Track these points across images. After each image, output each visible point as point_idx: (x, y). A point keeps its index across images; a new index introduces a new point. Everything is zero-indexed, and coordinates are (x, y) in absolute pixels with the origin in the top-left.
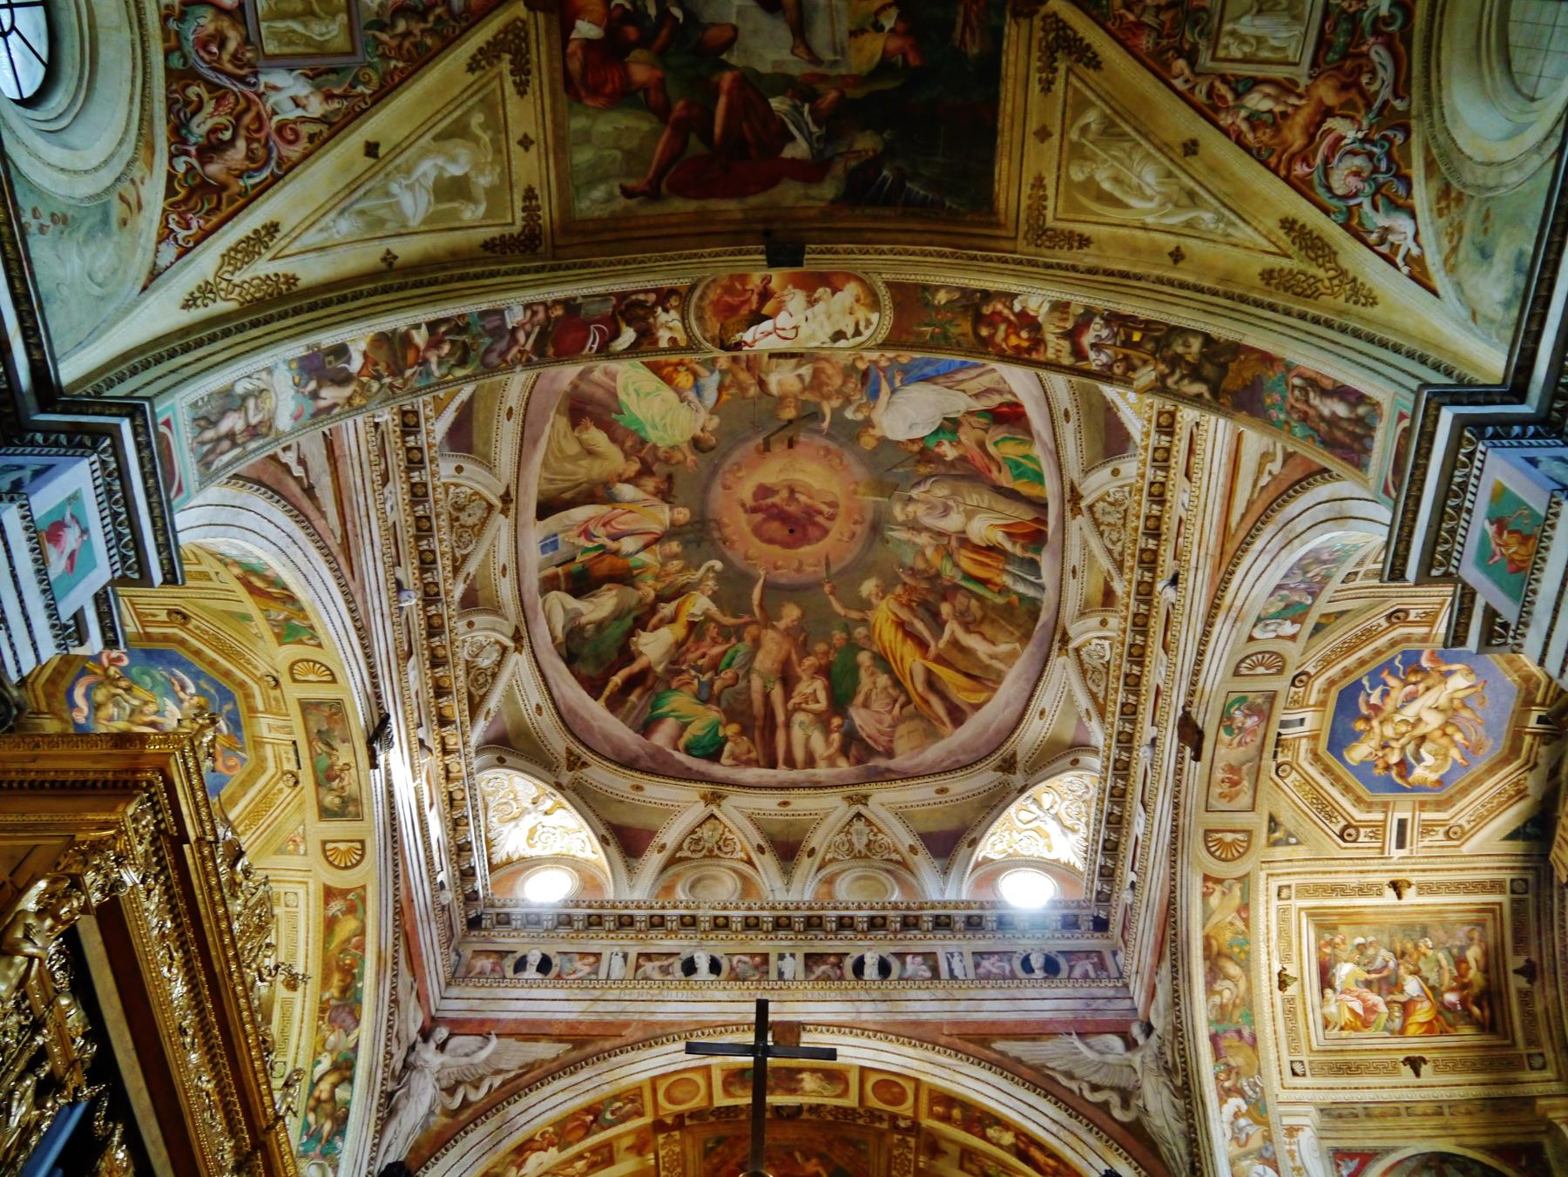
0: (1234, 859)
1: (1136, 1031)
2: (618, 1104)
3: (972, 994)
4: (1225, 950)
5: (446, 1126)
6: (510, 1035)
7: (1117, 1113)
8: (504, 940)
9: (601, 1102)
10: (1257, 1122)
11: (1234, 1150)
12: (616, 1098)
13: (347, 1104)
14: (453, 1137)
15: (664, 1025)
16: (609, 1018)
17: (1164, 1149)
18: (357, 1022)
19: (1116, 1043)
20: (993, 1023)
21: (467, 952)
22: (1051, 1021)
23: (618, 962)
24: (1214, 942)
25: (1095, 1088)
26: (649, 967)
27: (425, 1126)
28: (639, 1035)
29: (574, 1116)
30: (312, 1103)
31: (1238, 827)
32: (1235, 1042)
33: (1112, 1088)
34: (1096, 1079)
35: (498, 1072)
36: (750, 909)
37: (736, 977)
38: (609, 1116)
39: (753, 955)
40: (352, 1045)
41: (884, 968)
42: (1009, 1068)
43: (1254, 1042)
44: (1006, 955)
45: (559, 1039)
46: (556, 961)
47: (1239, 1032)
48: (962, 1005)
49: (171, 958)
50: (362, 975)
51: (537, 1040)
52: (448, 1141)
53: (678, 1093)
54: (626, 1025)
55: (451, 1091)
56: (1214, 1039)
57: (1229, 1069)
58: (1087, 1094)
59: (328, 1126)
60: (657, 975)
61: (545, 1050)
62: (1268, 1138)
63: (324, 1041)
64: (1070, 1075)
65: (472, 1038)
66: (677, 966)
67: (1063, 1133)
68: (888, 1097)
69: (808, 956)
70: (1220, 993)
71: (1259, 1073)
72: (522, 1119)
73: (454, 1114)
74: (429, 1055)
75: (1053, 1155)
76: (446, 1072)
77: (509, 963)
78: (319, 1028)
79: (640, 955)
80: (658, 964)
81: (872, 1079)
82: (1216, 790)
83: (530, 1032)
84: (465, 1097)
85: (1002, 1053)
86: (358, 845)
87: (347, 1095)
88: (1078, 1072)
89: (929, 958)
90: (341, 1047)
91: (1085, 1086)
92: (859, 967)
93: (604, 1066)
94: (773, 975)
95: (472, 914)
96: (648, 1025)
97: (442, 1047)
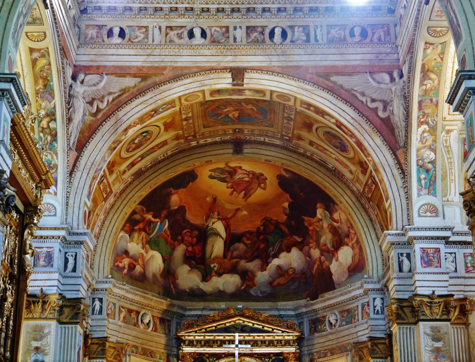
0: (440, 36)
1: (396, 74)
2: (164, 106)
3: (324, 51)
4: (431, 69)
5: (92, 121)
6: (112, 74)
7: (381, 114)
8: (101, 20)
9: (158, 107)
10: (431, 134)
11: (420, 145)
12: (163, 105)
13: (55, 129)
14: (97, 128)
15: (182, 68)
16: (156, 65)
17: (396, 131)
18: (53, 98)
19: (386, 77)
20: (332, 67)
21: (83, 27)
22: (359, 66)
23: (157, 31)
24: (426, 66)
25: (373, 101)
26: (172, 34)
27: (83, 120)
28: (171, 74)
29: (147, 114)
30: (40, 129)
31: (443, 26)
32: (429, 103)
33: (380, 101)
34: (374, 96)
35: (110, 94)
36: (219, 4)
37: (214, 42)
38: (161, 110)
39: (221, 27)
40: (53, 106)
41: (284, 34)
42: (335, 91)
43: (437, 105)
44: (344, 27)
45: (135, 76)
46: (127, 31)
47: (431, 100)
48: (319, 58)
49: (14, 154)
50: (52, 80)
51: (125, 77)
52: (96, 131)
53: (190, 99)
54: (164, 68)
55: (91, 103)
56: (420, 103)
57: (424, 114)
58: (370, 104)
59: (49, 138)
60: (176, 40)
61: (129, 82)
62: (435, 141)
63: (40, 106)
64: (363, 94)
65: (95, 76)
66: (185, 34)
67: (355, 124)
68: (283, 99)
69: (248, 28)
70: (426, 85)
71: (437, 116)
72: (125, 118)
73: (95, 115)
74: (79, 89)
75: (350, 131)
76: (87, 93)
77: (105, 32)
78: (37, 101)
79: (167, 27)
80: (176, 32)
81: (276, 94)
82: (434, 14)
83: (121, 72)
84: (98, 107)
85: (335, 83)
86: (43, 34)
87: (55, 126)
88: (367, 93)
89: (306, 28)
90: (48, 107)
91: (369, 100)
92: (272, 34)
93: (157, 91)
94: (231, 39)
95: (82, 8)
96: (175, 68)
97: (82, 82)
